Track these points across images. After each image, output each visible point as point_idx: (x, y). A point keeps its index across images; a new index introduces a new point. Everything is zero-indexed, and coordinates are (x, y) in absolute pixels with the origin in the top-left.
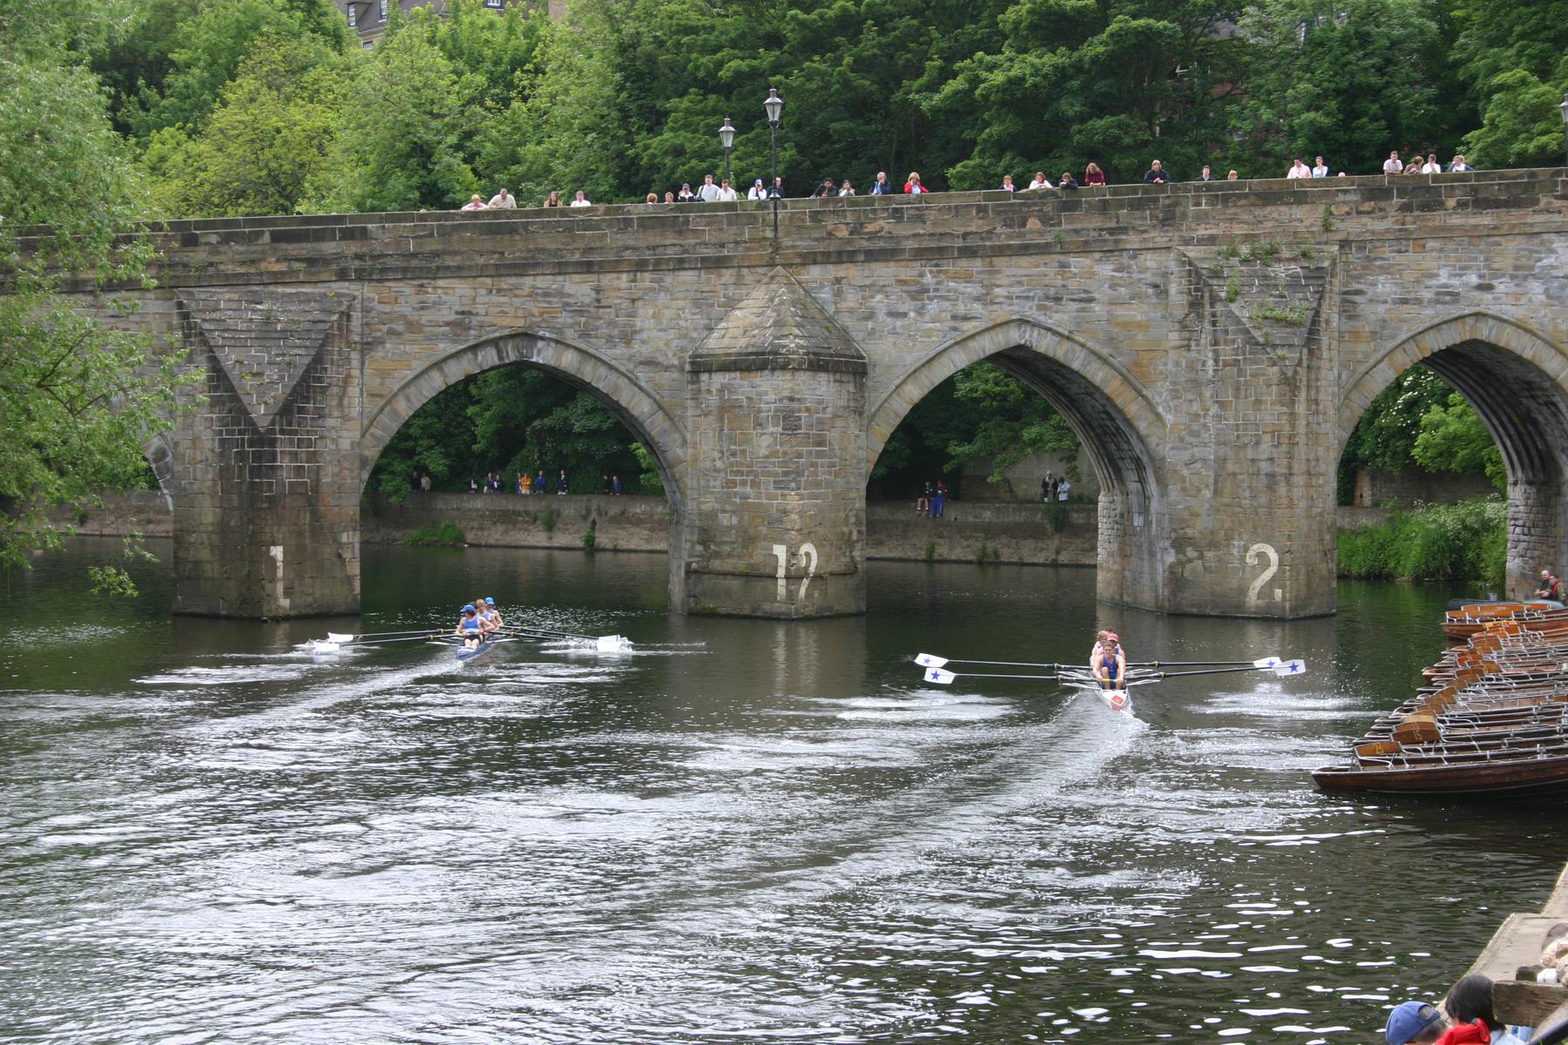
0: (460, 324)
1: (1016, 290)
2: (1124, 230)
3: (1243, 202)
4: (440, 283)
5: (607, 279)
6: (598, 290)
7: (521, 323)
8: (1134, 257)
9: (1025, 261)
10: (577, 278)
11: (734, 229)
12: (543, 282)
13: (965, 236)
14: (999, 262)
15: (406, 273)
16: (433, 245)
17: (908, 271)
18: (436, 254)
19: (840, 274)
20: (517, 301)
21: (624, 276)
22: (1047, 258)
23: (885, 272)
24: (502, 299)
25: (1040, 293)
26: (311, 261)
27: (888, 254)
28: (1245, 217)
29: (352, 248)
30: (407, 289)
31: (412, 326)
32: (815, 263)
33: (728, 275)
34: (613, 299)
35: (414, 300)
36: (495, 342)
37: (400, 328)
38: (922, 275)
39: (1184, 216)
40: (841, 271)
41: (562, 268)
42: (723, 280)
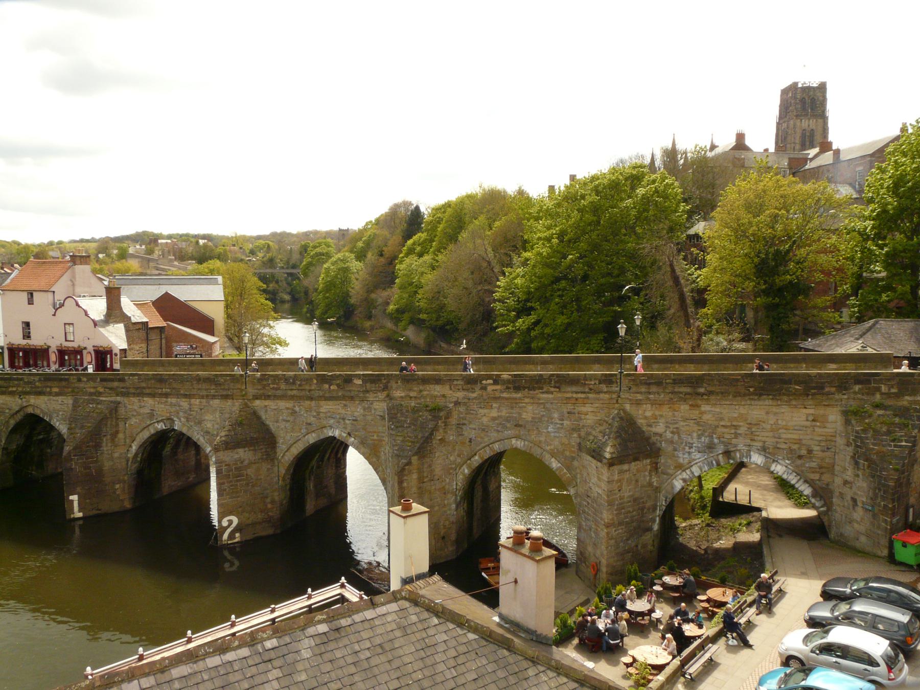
0: (151, 415)
1: (329, 414)
2: (367, 391)
3: (415, 382)
4: (145, 399)
5: (193, 401)
6: (190, 405)
7: (168, 415)
8: (372, 404)
9: (330, 403)
10: (184, 400)
11: (232, 384)
12: (174, 400)
13: (310, 391)
14: (322, 403)
15: (134, 395)
16: (143, 385)
17: (289, 404)
18: (144, 388)
19: (266, 404)
20: (167, 407)
21: (198, 400)
22: (339, 402)
23: (282, 404)
24: (163, 406)
25: (338, 417)
26: (111, 389)
27: (283, 397)
28: (416, 389)
29: (121, 384)
30: (135, 400)
31: (139, 414)
32: (257, 399)
33: (230, 402)
34: (196, 408)
35: (138, 404)
36: (162, 421)
37: (135, 414)
38: (294, 406)
39: (392, 387)
40: (267, 403)
41: (178, 395)
42: (229, 403)
